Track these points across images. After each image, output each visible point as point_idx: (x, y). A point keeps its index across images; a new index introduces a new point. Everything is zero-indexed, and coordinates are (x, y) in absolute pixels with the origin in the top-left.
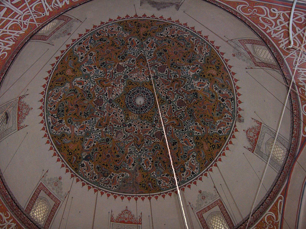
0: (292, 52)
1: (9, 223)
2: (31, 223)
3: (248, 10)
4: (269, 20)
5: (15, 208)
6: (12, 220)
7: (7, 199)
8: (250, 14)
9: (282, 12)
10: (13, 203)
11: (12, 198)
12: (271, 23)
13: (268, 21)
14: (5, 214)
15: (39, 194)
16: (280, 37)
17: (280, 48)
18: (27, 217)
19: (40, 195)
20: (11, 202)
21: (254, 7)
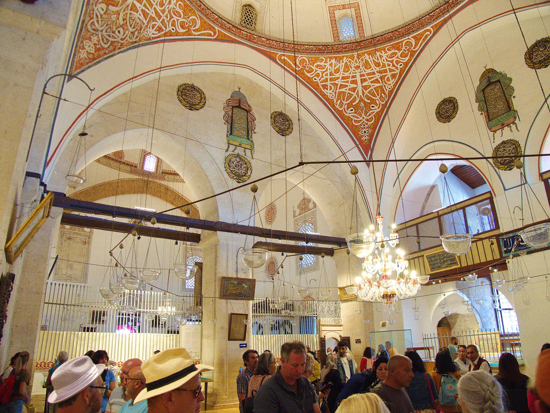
1: (328, 64)
2: (346, 45)
5: (324, 48)
6: (328, 59)
7: (311, 51)
10: (319, 47)
11: (314, 46)
14: (320, 61)
15: (335, 16)
18: (339, 44)
19: (337, 15)
20: (316, 48)
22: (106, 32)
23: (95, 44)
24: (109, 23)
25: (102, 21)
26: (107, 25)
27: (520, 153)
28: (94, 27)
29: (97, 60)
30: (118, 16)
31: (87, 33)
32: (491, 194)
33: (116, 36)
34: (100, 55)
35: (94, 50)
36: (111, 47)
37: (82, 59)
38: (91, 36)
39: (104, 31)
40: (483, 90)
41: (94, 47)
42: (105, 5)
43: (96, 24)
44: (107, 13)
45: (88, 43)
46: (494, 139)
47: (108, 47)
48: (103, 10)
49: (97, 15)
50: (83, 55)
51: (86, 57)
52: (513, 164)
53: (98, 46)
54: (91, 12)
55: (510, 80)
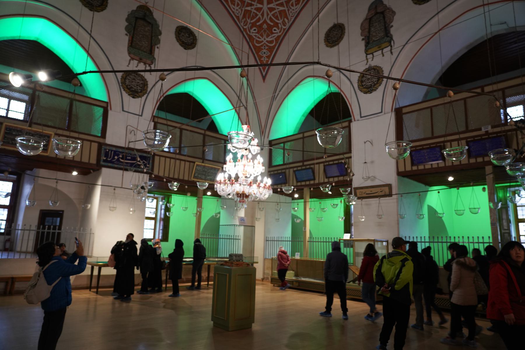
27: (146, 91)
32: (107, 106)
40: (137, 18)
46: (129, 64)
52: (137, 95)
55: (160, 33)
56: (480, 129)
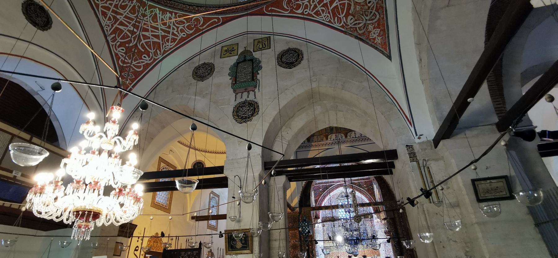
0: (149, 12)
3: (196, 23)
4: (181, 24)
8: (193, 20)
9: (180, 37)
12: (177, 23)
13: (180, 23)
16: (164, 17)
17: (156, 7)
21: (195, 29)
22: (367, 16)
23: (374, 28)
24: (361, 12)
25: (359, 20)
26: (363, 15)
28: (362, 26)
29: (386, 27)
30: (357, 4)
31: (365, 34)
33: (372, 6)
34: (383, 24)
35: (378, 29)
36: (379, 11)
37: (381, 42)
38: (368, 30)
39: (367, 18)
41: (376, 29)
42: (349, 17)
43: (361, 25)
44: (354, 15)
45: (372, 34)
47: (379, 14)
48: (352, 19)
49: (355, 25)
50: (379, 40)
51: (381, 37)
53: (376, 25)
54: (352, 30)
56: (11, 172)
